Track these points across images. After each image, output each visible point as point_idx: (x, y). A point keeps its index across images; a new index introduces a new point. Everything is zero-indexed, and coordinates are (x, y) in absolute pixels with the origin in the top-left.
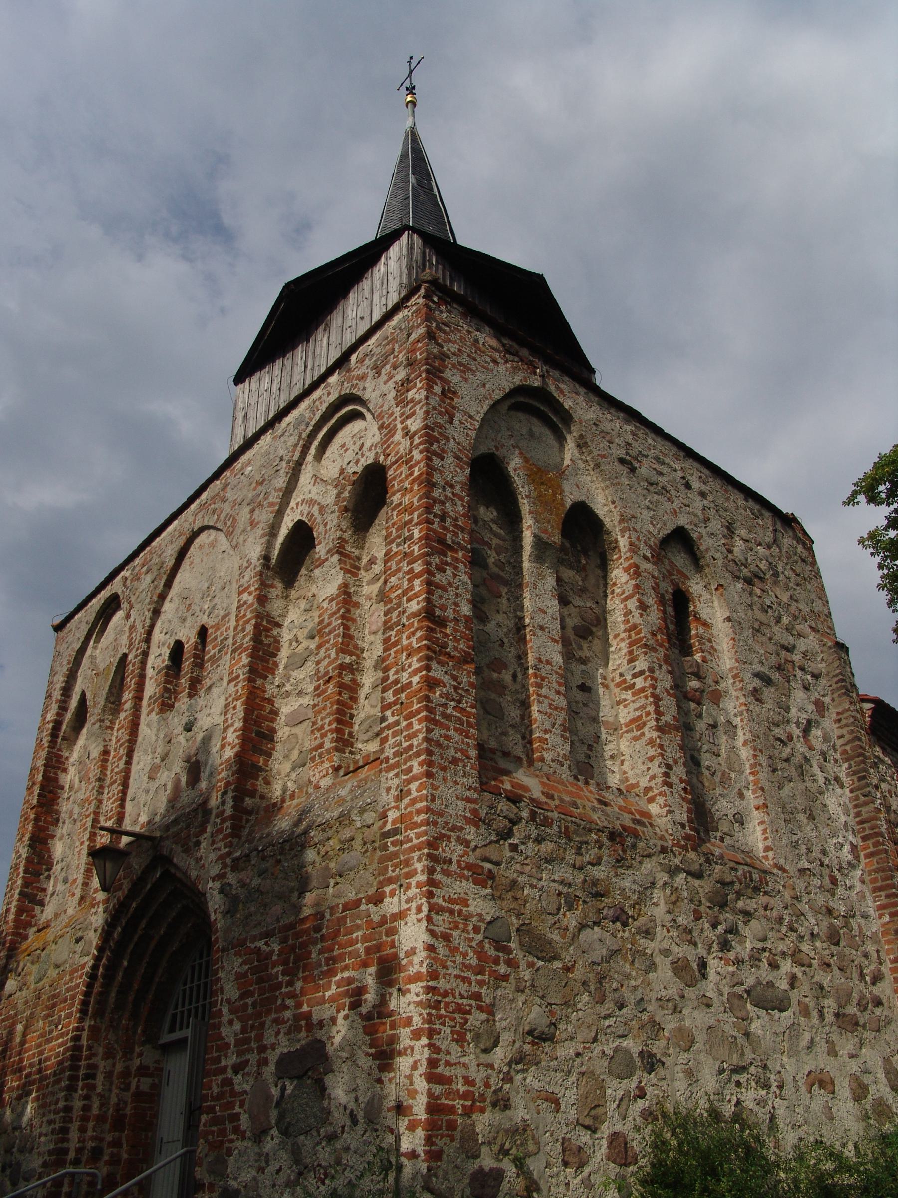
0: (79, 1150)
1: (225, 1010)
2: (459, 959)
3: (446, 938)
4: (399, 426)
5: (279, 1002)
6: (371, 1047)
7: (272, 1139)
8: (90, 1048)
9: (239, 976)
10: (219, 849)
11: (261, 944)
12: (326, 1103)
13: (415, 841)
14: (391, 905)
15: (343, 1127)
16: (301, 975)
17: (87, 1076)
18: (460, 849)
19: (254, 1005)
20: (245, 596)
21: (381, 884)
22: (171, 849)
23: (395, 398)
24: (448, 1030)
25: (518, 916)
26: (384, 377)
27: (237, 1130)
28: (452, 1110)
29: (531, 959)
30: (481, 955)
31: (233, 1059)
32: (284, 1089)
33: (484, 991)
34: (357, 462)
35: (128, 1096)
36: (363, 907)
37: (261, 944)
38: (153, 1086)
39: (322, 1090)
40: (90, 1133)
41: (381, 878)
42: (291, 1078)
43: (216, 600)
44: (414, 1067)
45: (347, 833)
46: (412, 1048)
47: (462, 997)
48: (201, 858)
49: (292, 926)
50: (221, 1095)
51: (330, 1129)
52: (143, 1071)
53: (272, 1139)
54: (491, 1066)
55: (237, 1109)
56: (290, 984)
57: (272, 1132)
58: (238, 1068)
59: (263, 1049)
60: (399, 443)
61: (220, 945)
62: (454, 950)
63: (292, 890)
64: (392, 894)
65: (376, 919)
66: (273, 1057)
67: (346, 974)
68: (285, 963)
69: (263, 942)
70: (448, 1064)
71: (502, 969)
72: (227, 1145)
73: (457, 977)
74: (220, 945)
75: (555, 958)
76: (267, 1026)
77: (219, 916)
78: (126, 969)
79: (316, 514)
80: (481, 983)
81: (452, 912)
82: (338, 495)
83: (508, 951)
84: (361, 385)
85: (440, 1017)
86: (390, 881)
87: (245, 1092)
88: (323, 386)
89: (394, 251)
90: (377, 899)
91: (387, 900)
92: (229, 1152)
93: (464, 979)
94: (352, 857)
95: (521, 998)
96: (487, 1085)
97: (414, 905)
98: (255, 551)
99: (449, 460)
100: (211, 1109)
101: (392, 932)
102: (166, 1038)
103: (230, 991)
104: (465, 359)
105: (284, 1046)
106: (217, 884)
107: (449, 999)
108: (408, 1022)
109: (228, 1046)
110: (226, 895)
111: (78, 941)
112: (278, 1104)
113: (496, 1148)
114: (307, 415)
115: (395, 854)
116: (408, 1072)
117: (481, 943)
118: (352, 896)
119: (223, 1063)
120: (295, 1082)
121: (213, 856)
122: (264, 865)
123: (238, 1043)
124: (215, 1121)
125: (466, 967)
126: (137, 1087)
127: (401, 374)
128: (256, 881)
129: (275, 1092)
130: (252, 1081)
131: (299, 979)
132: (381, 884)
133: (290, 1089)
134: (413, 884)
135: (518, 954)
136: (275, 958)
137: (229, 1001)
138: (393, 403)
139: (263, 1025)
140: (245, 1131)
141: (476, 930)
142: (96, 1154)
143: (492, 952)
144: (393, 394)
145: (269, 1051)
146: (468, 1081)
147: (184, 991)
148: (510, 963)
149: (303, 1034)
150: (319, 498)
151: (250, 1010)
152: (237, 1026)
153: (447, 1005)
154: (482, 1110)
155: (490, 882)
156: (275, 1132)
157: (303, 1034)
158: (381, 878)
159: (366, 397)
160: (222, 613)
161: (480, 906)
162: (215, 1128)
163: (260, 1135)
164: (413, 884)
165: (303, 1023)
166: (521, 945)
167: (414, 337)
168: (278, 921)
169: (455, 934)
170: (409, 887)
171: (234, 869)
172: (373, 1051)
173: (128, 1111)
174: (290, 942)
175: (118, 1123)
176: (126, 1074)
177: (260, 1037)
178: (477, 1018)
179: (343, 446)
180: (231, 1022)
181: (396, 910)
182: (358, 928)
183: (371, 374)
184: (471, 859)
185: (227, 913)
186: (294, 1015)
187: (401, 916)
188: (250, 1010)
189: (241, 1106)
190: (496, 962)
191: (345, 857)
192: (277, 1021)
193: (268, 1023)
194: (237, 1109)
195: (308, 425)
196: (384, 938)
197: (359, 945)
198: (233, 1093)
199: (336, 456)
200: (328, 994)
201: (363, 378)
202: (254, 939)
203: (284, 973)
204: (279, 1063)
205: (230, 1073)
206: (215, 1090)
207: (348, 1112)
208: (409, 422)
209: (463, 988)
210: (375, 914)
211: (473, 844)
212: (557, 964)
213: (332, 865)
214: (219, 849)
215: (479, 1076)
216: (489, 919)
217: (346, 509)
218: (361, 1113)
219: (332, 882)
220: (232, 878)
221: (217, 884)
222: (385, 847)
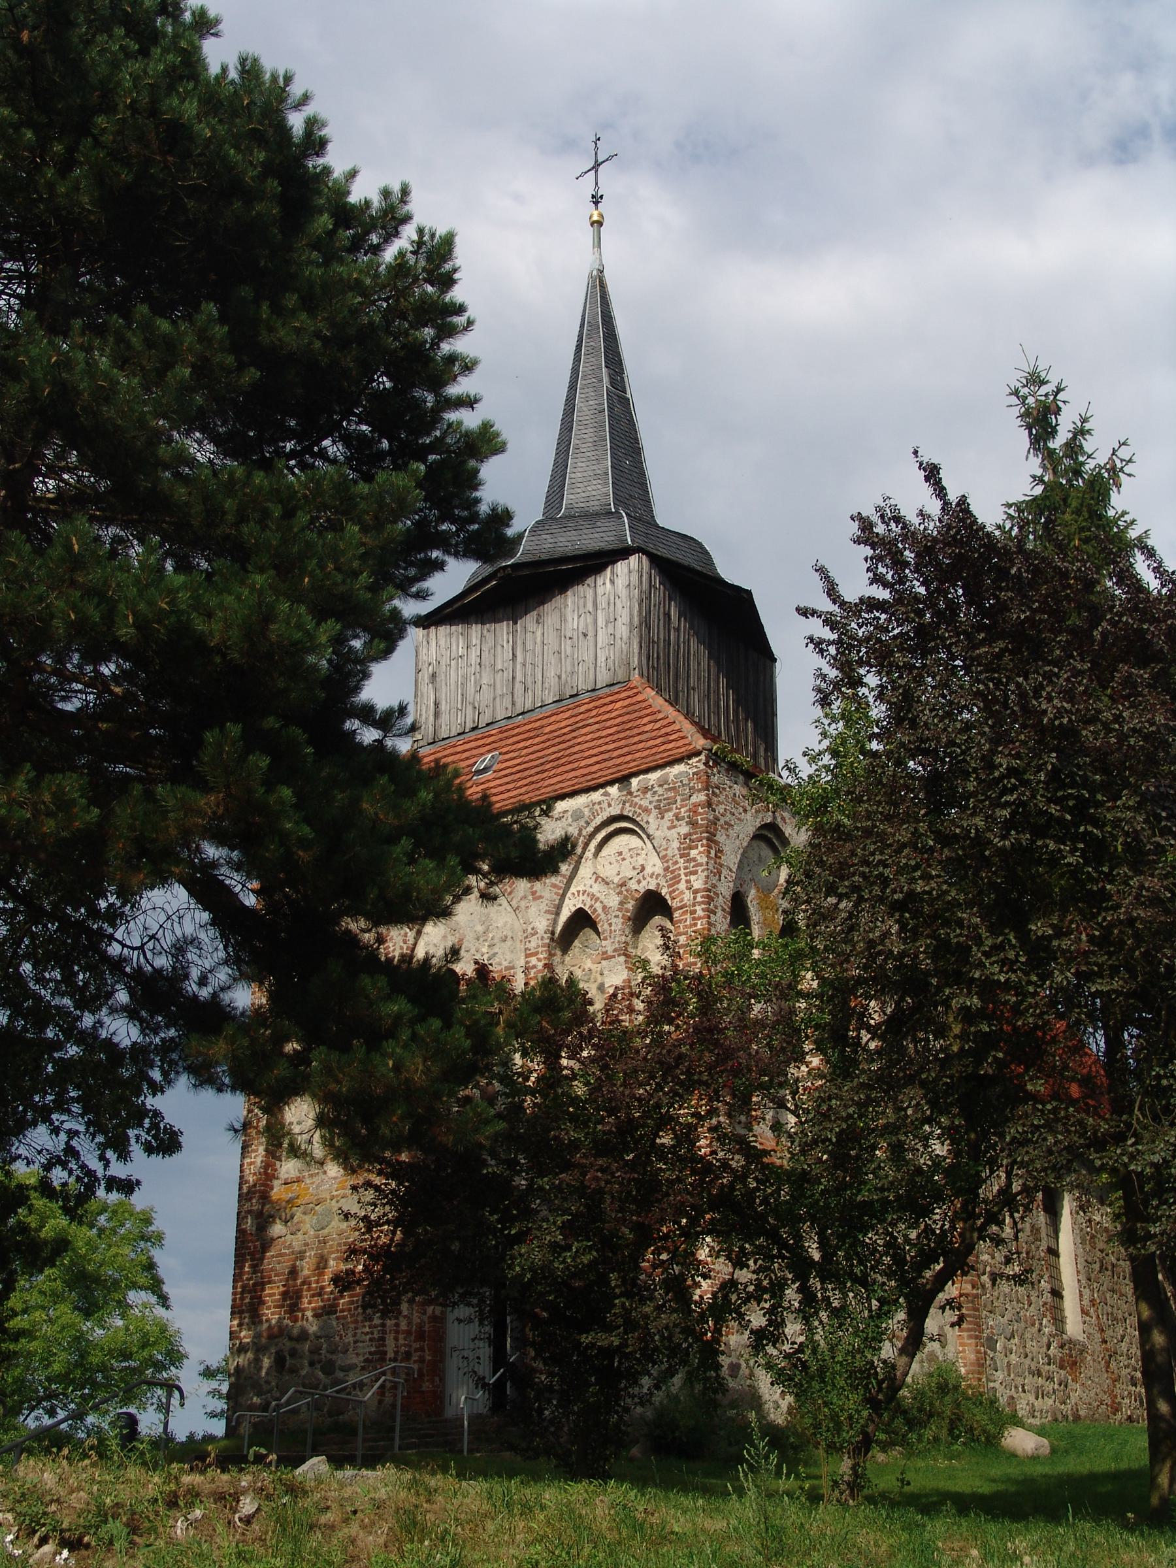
0: (396, 1353)
4: (683, 876)
20: (533, 961)
23: (679, 849)
26: (666, 823)
34: (639, 882)
35: (425, 1318)
38: (442, 1312)
40: (401, 1342)
43: (496, 949)
60: (682, 893)
79: (600, 910)
82: (621, 903)
84: (644, 816)
88: (601, 791)
89: (621, 567)
98: (542, 924)
99: (720, 913)
104: (728, 817)
114: (586, 812)
127: (684, 829)
138: (677, 852)
142: (408, 1356)
144: (676, 844)
150: (602, 898)
159: (651, 832)
160: (505, 964)
167: (694, 799)
175: (420, 1336)
179: (620, 853)
183: (655, 812)
195: (588, 823)
199: (613, 860)
201: (647, 811)
208: (693, 878)
217: (629, 919)
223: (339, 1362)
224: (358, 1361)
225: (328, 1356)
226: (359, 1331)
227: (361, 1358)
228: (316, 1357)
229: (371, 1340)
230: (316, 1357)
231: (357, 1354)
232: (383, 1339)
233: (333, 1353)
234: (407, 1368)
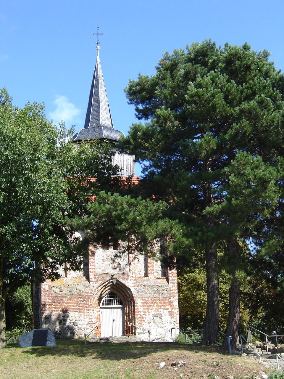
1: (139, 306)
36: (167, 299)
37: (147, 299)
45: (164, 288)
59: (149, 313)
66: (151, 314)
77: (135, 293)
91: (171, 299)
105: (153, 313)
106: (133, 288)
108: (176, 313)
124: (140, 320)
128: (143, 290)
188: (145, 307)
189: (145, 319)
194: (144, 319)
198: (143, 317)
204: (152, 315)
205: (142, 315)
210: (170, 300)
220: (136, 287)
221: (133, 288)
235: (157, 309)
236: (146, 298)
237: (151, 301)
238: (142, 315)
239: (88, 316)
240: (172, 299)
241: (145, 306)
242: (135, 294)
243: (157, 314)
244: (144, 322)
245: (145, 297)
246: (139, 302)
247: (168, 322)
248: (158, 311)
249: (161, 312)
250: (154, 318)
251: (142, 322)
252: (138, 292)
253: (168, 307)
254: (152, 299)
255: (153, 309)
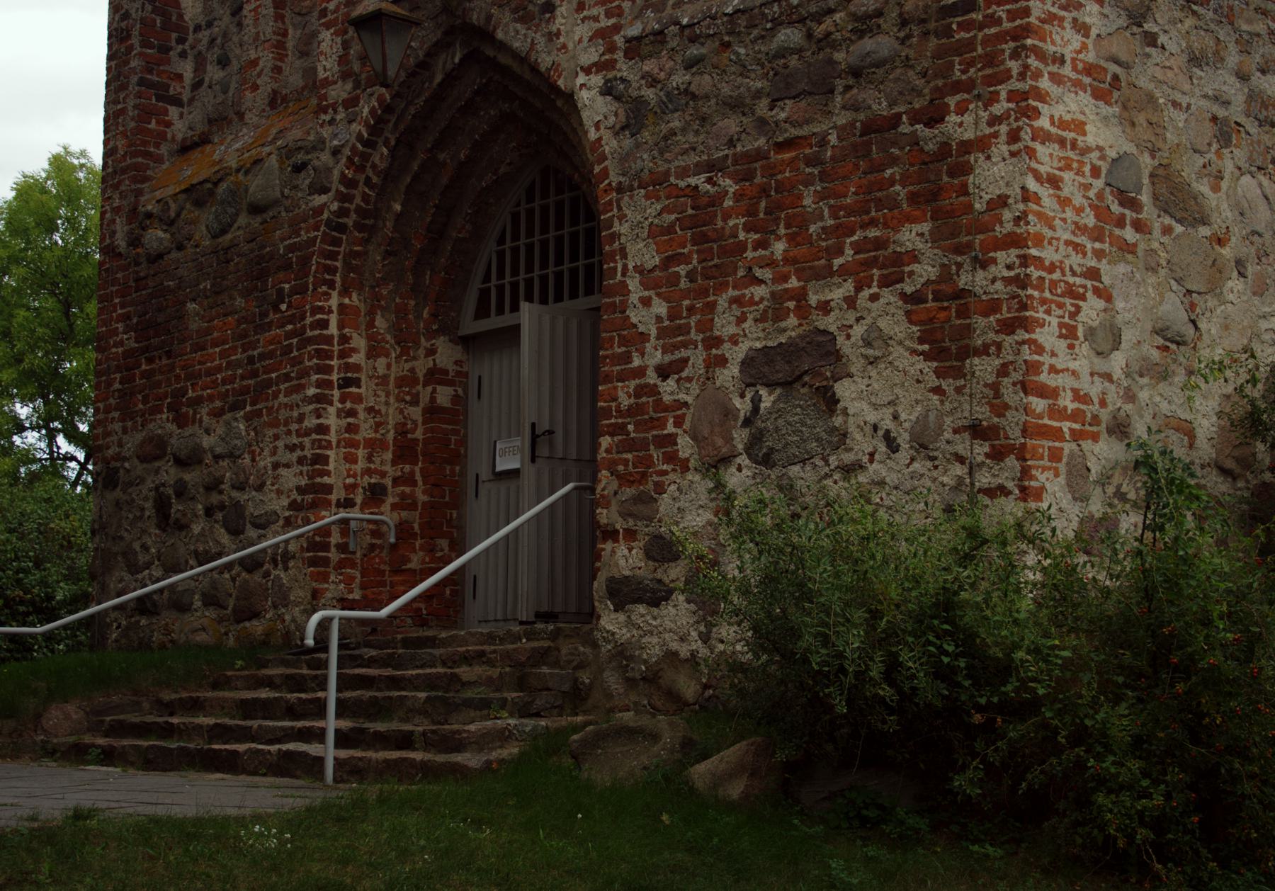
1: (633, 284)
2: (1069, 214)
3: (1054, 182)
5: (741, 273)
6: (921, 341)
7: (740, 469)
8: (344, 339)
9: (655, 232)
10: (596, 19)
11: (698, 180)
12: (838, 421)
13: (1007, 25)
14: (962, 125)
15: (872, 455)
16: (782, 231)
17: (346, 383)
18: (1076, 41)
19: (691, 276)
21: (940, 93)
22: (489, 17)
24: (1055, 321)
25: (1153, 153)
27: (671, 458)
28: (1057, 434)
29: (1167, 220)
30: (1101, 212)
31: (656, 357)
32: (756, 401)
33: (1104, 266)
35: (416, 413)
36: (905, 128)
37: (698, 180)
38: (456, 398)
39: (831, 402)
41: (940, 83)
42: (770, 385)
44: (1003, 371)
46: (999, 346)
47: (1074, 274)
48: (558, 34)
49: (759, 155)
50: (632, 411)
51: (848, 458)
52: (436, 376)
53: (740, 469)
54: (1108, 377)
55: (670, 429)
56: (762, 244)
57: (738, 460)
58: (664, 372)
59: (713, 342)
61: (614, 178)
62: (1064, 202)
63: (758, 95)
64: (961, 110)
65: (931, 147)
66: (737, 354)
67: (873, 233)
68: (751, 212)
69: (703, 177)
70: (1053, 370)
71: (1129, 234)
72: (656, 478)
73: (1068, 243)
74: (614, 178)
75: (1204, 221)
76: (720, 309)
77: (607, 135)
78: (399, 216)
80: (1099, 254)
81: (1062, 142)
83: (1134, 205)
85: (1044, 301)
86: (957, 87)
87: (686, 404)
90: (934, 117)
91: (953, 118)
92: (660, 488)
93: (1078, 248)
94: (881, 44)
95: (1152, 279)
96: (1103, 403)
97: (1004, 129)
100: (622, 429)
101: (967, 169)
102: (470, 326)
103: (643, 254)
105: (754, 339)
106: (597, 80)
107: (1057, 275)
108: (992, 307)
109: (644, 337)
110: (618, 98)
111: (298, 169)
112: (747, 422)
113: (1110, 490)
115: (970, 45)
116: (991, 379)
117: (1100, 196)
118: (881, 108)
119: (637, 362)
120: (778, 391)
121: (584, 31)
122: (694, 51)
123: (662, 333)
124: (629, 445)
125: (1079, 228)
126: (433, 399)
129: (742, 406)
130: (695, 388)
131: (779, 238)
132: (940, 93)
133: (767, 400)
134: (1003, 95)
135: (1149, 212)
136: (728, 203)
137: (639, 270)
139: (711, 307)
140: (687, 460)
141: (1096, 172)
143: (1116, 208)
145: (727, 345)
146: (1078, 396)
147: (501, 255)
148: (1139, 226)
149: (792, 321)
151: (684, 283)
152: (660, 308)
153: (1054, 284)
154: (1095, 438)
155: (1116, 94)
156: (743, 460)
157: (792, 321)
158: (940, 83)
161: (1103, 133)
162: (629, 456)
163: (717, 464)
164: (1003, 95)
165: (791, 304)
166: (1156, 197)
168: (731, 143)
169: (1067, 176)
170: (994, 98)
171: (629, 55)
172: (926, 347)
173: (419, 434)
174: (758, 180)
176: (407, 381)
177: (706, 326)
178: (1092, 309)
180: (646, 302)
181: (969, 135)
182: (894, 161)
184: (1091, 57)
185: (623, 128)
186: (773, 294)
187: (982, 144)
188: (684, 283)
189: (678, 423)
190: (1120, 223)
191: (868, 44)
192: (736, 301)
193: (722, 302)
194: (670, 429)
196: (945, 179)
197: (898, 188)
198: (659, 405)
200: (837, 262)
202: (684, 173)
203: (748, 228)
204: (746, 364)
205: (652, 378)
206: (625, 402)
207: (881, 433)
209: (1075, 260)
211: (1094, 32)
212: (1204, 231)
213: (839, 56)
214: (596, 19)
215: (1094, 389)
216: (1114, 155)
218: (906, 436)
219: (839, 84)
220: (624, 68)
221: (597, 80)
222: (948, 32)
223: (250, 509)
224: (279, 505)
225: (235, 494)
226: (280, 444)
227: (285, 502)
228: (215, 499)
229: (301, 461)
230: (215, 499)
231: (279, 492)
232: (322, 459)
233: (241, 487)
234: (375, 522)
235: (794, 283)
236: (699, 169)
237: (738, 197)
238: (652, 378)
239: (295, 440)
240: (962, 125)
241: (682, 270)
242: (610, 145)
243: (788, 351)
244: (671, 458)
245: (694, 158)
246: (635, 234)
247: (903, 439)
248: (803, 311)
249: (830, 323)
250: (767, 400)
251: (648, 461)
252: (635, 117)
253: (911, 236)
254: (748, 176)
255: (759, 291)
